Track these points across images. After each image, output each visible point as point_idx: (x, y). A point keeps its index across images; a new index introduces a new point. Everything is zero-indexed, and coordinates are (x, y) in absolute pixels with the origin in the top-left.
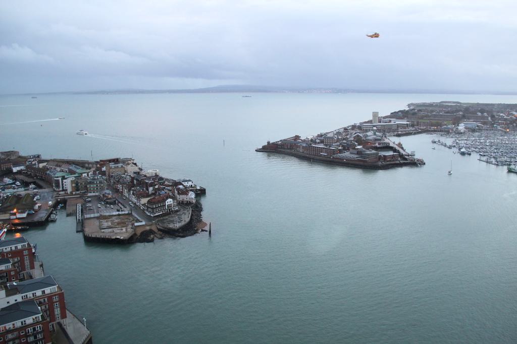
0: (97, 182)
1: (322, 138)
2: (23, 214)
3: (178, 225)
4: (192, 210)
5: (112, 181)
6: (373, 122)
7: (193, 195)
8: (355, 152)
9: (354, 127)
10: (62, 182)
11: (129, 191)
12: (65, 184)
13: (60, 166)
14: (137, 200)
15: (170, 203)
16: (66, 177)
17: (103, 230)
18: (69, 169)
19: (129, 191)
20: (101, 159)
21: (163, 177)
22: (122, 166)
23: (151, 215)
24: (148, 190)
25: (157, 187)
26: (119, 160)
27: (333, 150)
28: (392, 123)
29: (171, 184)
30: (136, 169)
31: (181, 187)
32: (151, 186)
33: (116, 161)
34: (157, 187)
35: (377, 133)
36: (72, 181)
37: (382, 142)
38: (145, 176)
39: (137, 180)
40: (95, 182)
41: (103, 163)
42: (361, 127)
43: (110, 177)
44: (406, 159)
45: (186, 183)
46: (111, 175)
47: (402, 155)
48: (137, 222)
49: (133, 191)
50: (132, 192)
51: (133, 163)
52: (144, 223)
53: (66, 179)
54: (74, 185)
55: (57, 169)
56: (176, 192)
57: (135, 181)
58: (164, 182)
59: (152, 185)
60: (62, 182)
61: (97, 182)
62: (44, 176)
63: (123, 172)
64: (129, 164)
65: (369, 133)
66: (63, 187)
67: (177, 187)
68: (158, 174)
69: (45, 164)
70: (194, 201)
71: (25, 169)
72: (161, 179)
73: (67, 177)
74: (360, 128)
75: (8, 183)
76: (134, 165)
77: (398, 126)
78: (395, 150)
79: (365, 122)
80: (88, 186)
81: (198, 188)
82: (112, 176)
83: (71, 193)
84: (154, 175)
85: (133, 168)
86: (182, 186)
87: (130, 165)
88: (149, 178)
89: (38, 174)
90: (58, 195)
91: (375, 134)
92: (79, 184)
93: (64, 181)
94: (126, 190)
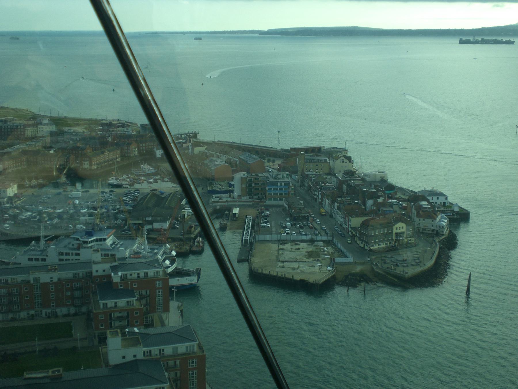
0: (281, 184)
2: (163, 224)
3: (411, 271)
4: (440, 248)
5: (306, 185)
7: (446, 221)
11: (333, 202)
13: (226, 153)
14: (345, 218)
15: (401, 230)
17: (281, 264)
18: (240, 159)
19: (333, 202)
20: (292, 147)
21: (394, 184)
22: (325, 161)
23: (366, 248)
24: (364, 204)
25: (380, 200)
26: (322, 150)
29: (407, 198)
30: (347, 166)
31: (424, 204)
32: (371, 198)
33: (317, 151)
34: (380, 200)
36: (241, 177)
38: (363, 180)
39: (349, 186)
40: (279, 184)
41: (295, 152)
43: (304, 177)
45: (435, 198)
46: (307, 173)
48: (340, 257)
49: (340, 203)
50: (337, 205)
51: (345, 157)
52: (351, 259)
54: (244, 185)
55: (221, 157)
56: (414, 212)
57: (345, 188)
58: (396, 193)
59: (374, 196)
61: (281, 184)
63: (327, 172)
64: (337, 158)
68: (385, 178)
69: (203, 148)
70: (446, 232)
72: (391, 187)
75: (147, 172)
76: (346, 160)
80: (267, 189)
81: (456, 209)
82: (307, 175)
83: (240, 197)
84: (378, 179)
85: (344, 164)
86: (427, 203)
87: (339, 160)
88: (371, 183)
90: (217, 199)
92: (253, 185)
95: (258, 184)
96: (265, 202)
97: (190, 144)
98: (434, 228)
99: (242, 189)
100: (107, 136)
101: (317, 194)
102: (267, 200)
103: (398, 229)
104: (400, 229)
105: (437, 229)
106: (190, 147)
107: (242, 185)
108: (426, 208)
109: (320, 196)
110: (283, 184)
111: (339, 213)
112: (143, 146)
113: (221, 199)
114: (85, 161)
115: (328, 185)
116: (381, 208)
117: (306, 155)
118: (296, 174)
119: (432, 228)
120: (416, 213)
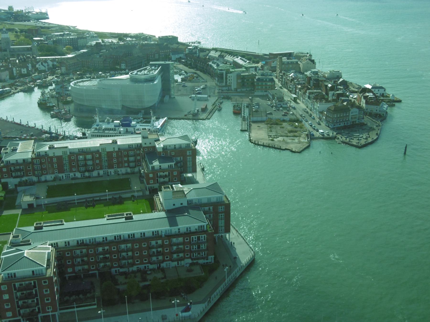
0: (266, 80)
10: (226, 76)
12: (228, 78)
16: (231, 70)
24: (327, 94)
33: (289, 55)
53: (231, 72)
54: (240, 81)
55: (220, 60)
57: (312, 82)
60: (226, 76)
62: (205, 68)
66: (226, 82)
67: (364, 95)
71: (184, 57)
73: (233, 70)
83: (236, 90)
86: (372, 94)
89: (199, 65)
92: (245, 80)
93: (229, 75)
94: (300, 92)
95: (249, 80)
96: (254, 93)
97: (198, 50)
98: (378, 112)
99: (238, 83)
100: (136, 45)
101: (292, 87)
102: (255, 92)
103: (353, 112)
104: (354, 113)
105: (380, 113)
106: (198, 52)
107: (237, 81)
108: (371, 97)
109: (294, 89)
110: (268, 80)
111: (310, 101)
112: (162, 53)
113: (222, 91)
114: (122, 63)
115: (300, 81)
116: (340, 98)
117: (283, 58)
118: (276, 73)
119: (376, 112)
120: (364, 101)
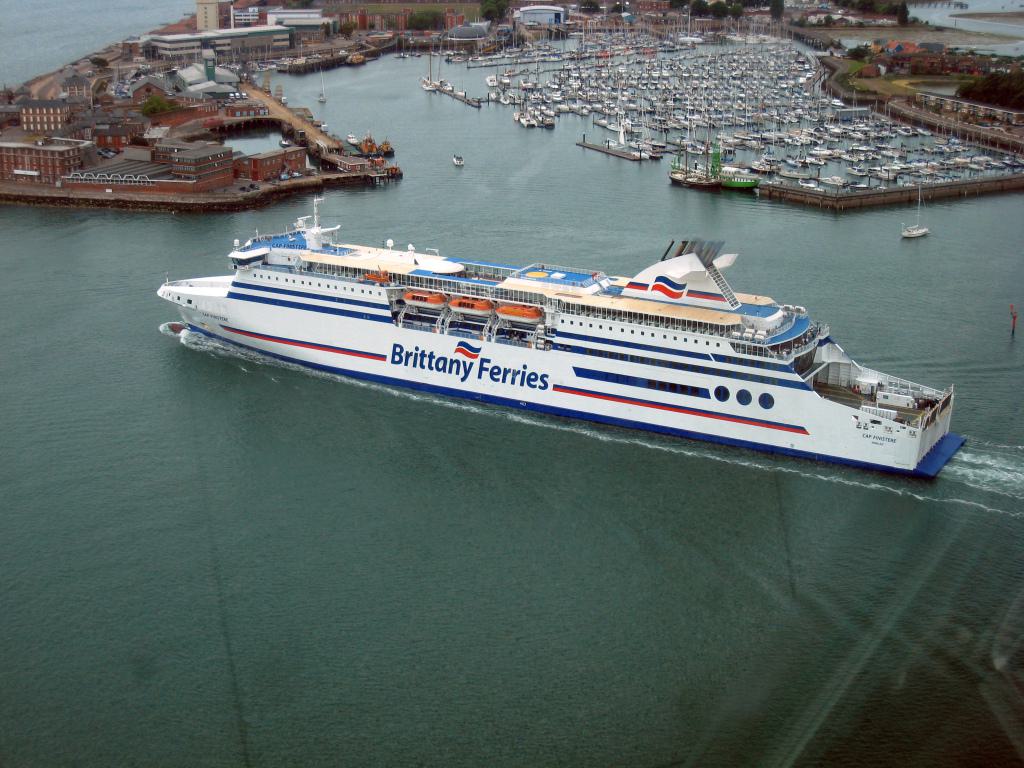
1: (13, 108)
6: (200, 25)
8: (143, 154)
9: (129, 50)
27: (61, 153)
28: (271, 24)
35: (218, 71)
37: (239, 104)
42: (155, 49)
44: (332, 167)
47: (319, 150)
65: (191, 74)
74: (151, 52)
77: (295, 35)
78: (289, 134)
79: (170, 29)
91: (210, 75)
